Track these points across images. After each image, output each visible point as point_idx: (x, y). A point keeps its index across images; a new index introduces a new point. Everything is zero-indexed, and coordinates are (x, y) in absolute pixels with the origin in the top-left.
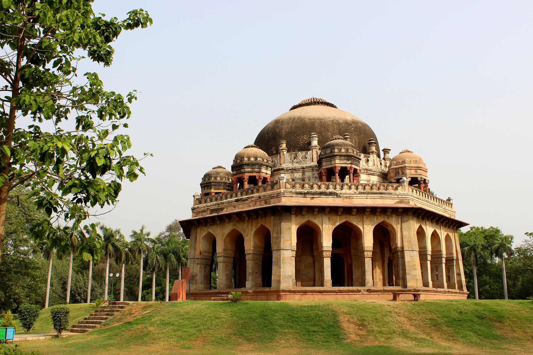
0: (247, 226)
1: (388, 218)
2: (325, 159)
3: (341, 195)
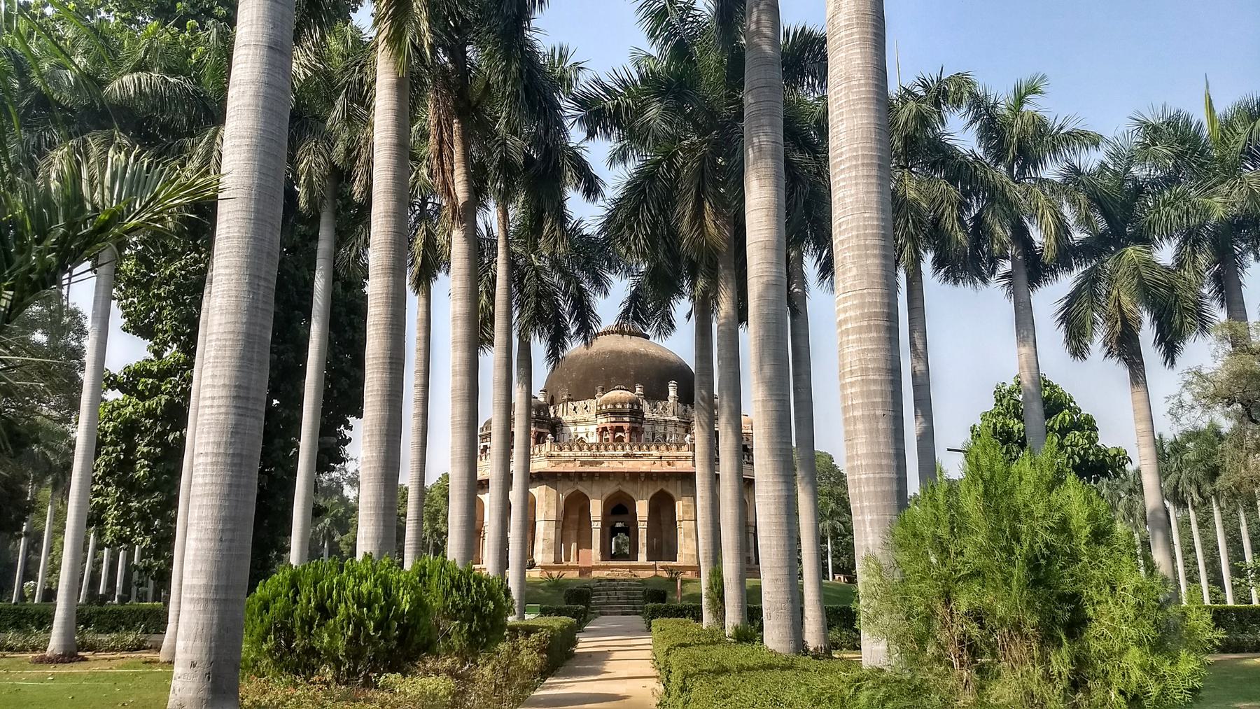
0: (642, 488)
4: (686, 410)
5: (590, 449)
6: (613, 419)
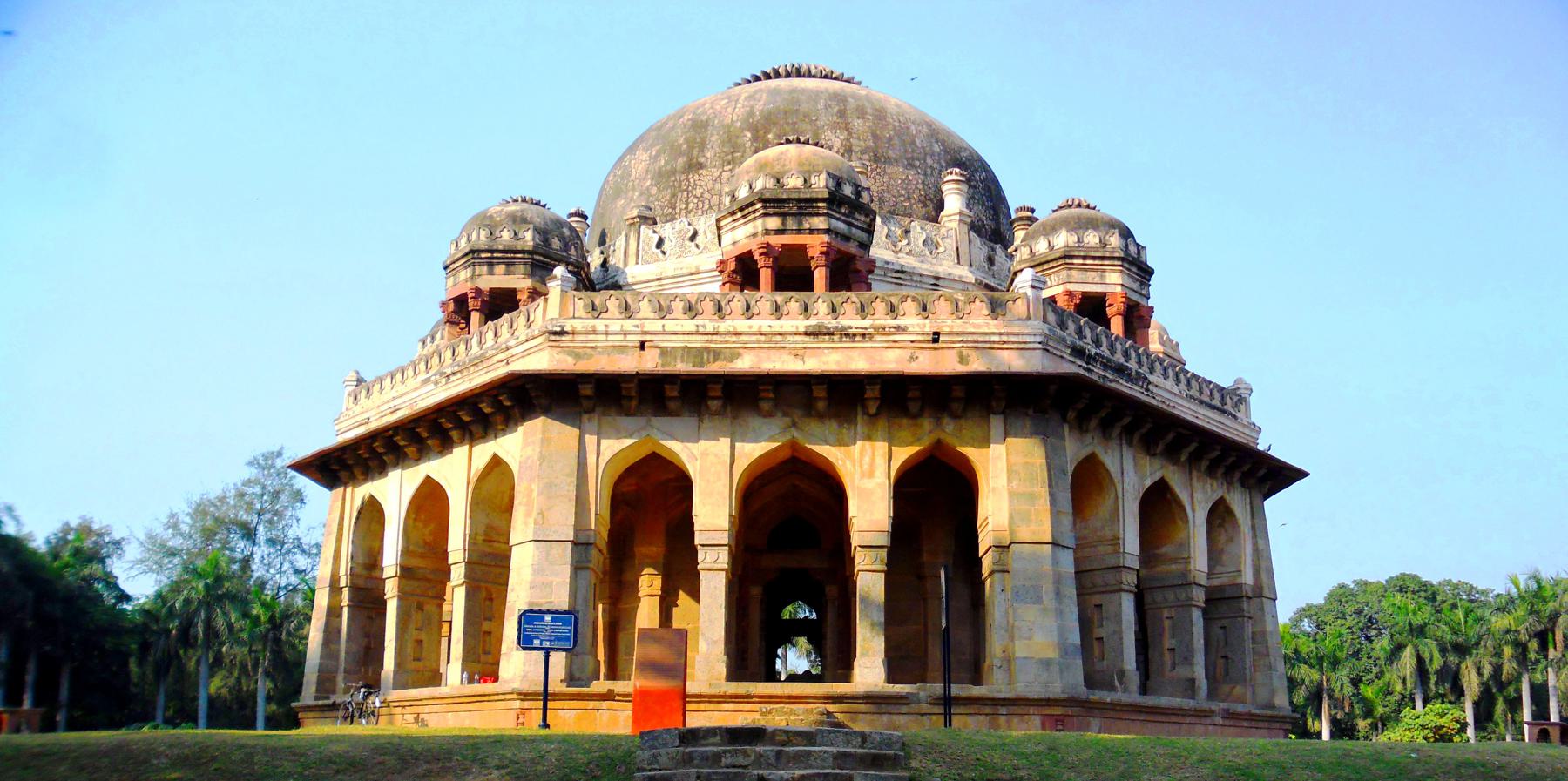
1: (1229, 491)
2: (1081, 261)
3: (1155, 390)
4: (991, 260)
5: (691, 310)
6: (774, 223)
